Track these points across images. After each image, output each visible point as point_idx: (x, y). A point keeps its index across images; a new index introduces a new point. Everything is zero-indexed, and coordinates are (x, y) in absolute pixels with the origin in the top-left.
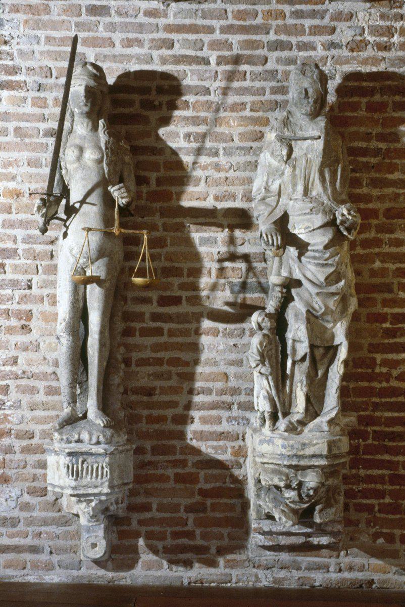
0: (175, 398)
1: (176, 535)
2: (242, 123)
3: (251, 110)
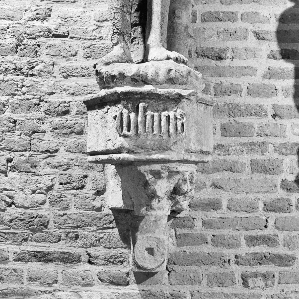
0: (251, 63)
1: (252, 241)
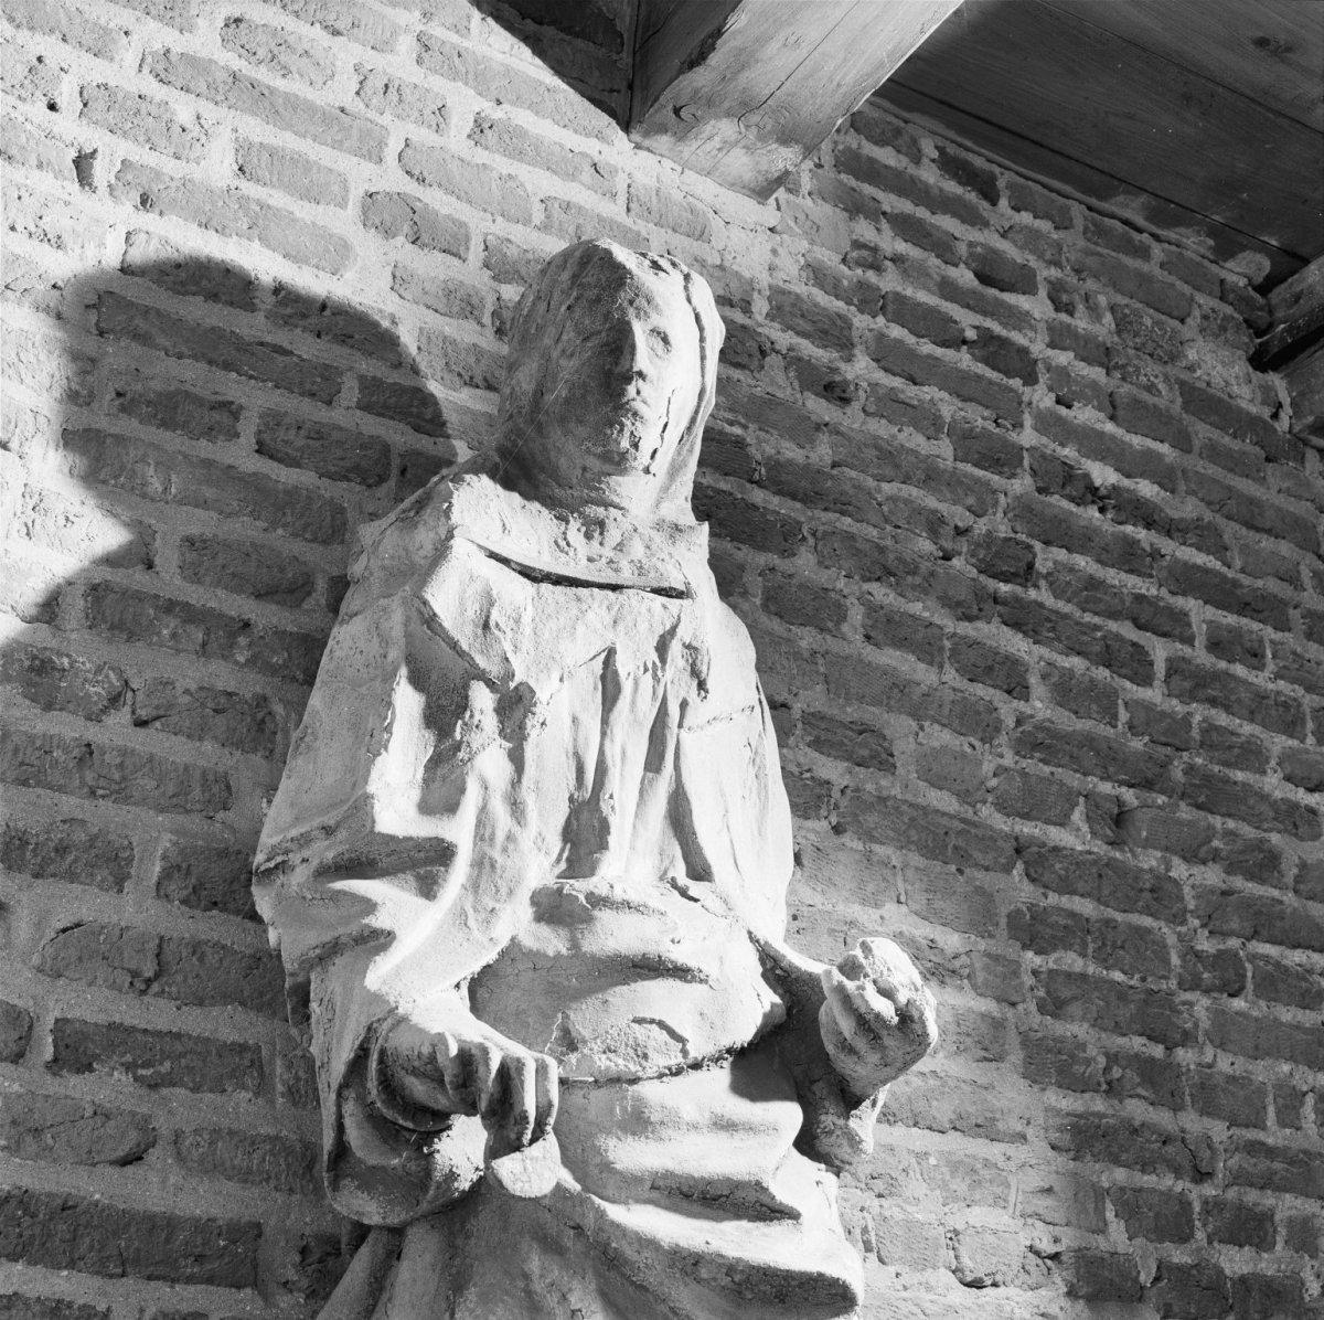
2: (209, 493)
3: (261, 450)
